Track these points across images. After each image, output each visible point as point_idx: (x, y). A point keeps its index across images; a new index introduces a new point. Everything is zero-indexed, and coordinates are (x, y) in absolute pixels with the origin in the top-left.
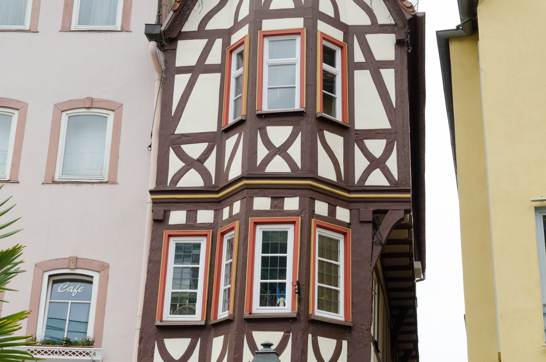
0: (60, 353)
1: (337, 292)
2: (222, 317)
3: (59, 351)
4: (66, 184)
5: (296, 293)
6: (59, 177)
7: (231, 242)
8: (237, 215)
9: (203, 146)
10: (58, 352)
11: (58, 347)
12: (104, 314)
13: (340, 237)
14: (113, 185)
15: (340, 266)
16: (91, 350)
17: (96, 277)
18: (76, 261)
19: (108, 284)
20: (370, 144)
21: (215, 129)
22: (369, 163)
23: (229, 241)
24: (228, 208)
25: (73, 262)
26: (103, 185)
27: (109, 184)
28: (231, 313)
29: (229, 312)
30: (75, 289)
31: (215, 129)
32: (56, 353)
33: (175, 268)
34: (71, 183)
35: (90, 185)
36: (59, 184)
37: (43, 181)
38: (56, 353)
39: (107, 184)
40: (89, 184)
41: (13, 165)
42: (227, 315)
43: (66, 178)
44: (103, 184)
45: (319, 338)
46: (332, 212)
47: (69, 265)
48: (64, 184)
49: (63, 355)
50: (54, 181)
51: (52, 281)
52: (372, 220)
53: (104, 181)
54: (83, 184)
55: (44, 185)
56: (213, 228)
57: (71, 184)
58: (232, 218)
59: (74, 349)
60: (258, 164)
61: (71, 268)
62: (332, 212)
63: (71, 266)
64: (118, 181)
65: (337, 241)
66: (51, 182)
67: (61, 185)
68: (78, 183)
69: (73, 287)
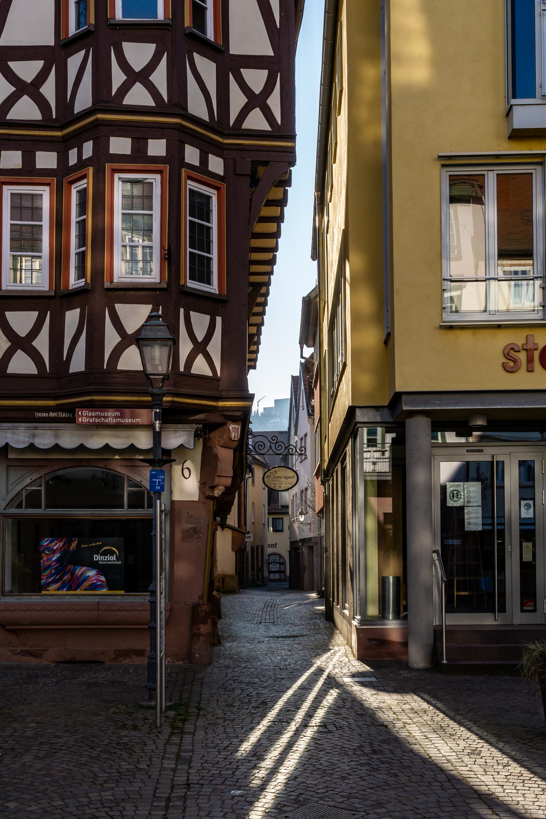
1: (209, 260)
2: (74, 287)
5: (166, 259)
7: (83, 193)
8: (89, 159)
9: (39, 65)
13: (213, 194)
15: (212, 228)
20: (248, 74)
21: (51, 42)
22: (247, 100)
23: (79, 192)
24: (75, 150)
28: (89, 281)
29: (86, 281)
31: (51, 42)
33: (11, 225)
42: (83, 284)
45: (193, 314)
46: (204, 161)
52: (250, 173)
56: (57, 175)
58: (82, 164)
60: (113, 94)
62: (204, 161)
65: (209, 198)
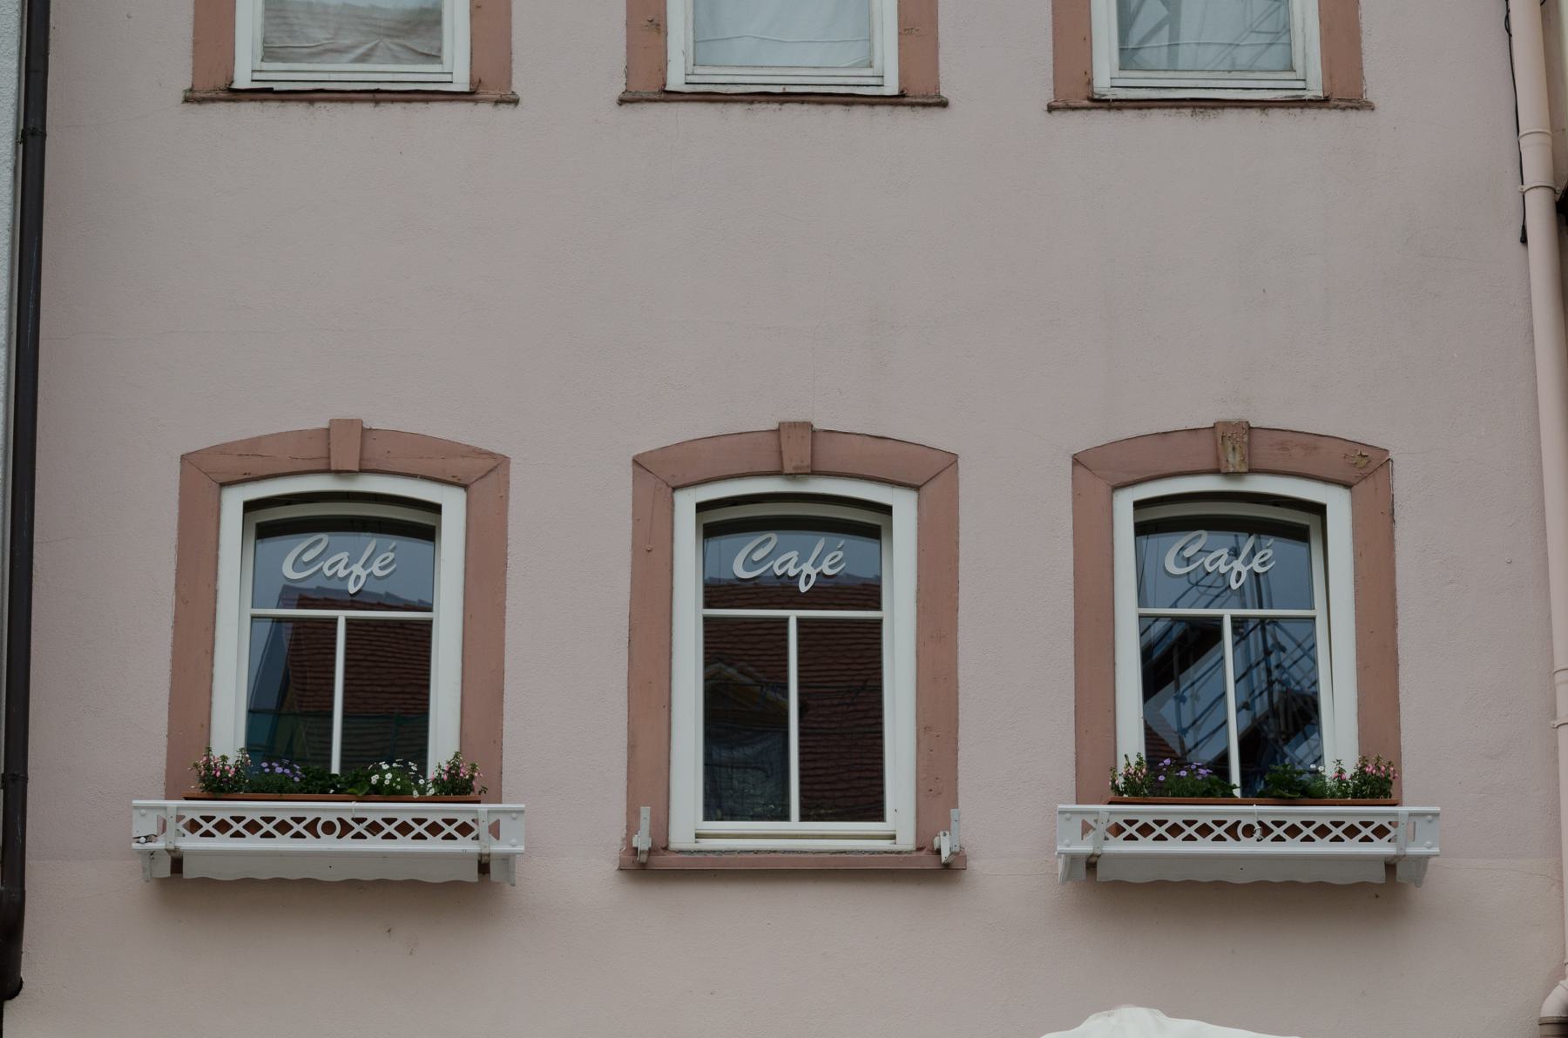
0: (1266, 830)
3: (1260, 823)
4: (1149, 108)
6: (687, 75)
10: (1257, 827)
11: (1255, 808)
12: (1396, 666)
14: (1353, 114)
16: (1395, 814)
17: (1338, 505)
18: (1246, 439)
19: (1397, 535)
25: (1237, 446)
26: (1310, 113)
27: (1336, 107)
30: (806, 561)
32: (1249, 830)
34: (1171, 107)
35: (1254, 115)
36: (1119, 108)
37: (1048, 96)
38: (1249, 830)
39: (1325, 111)
40: (1248, 110)
41: (905, 30)
43: (1140, 83)
44: (1310, 107)
47: (1218, 459)
48: (1140, 108)
49: (1278, 839)
50: (1096, 97)
51: (254, 527)
53: (1308, 95)
54: (1223, 108)
55: (1056, 113)
57: (1174, 111)
59: (1321, 813)
61: (1231, 470)
63: (1231, 459)
64: (1369, 96)
66: (1086, 103)
67: (1129, 115)
68: (1201, 107)
69: (347, 554)
